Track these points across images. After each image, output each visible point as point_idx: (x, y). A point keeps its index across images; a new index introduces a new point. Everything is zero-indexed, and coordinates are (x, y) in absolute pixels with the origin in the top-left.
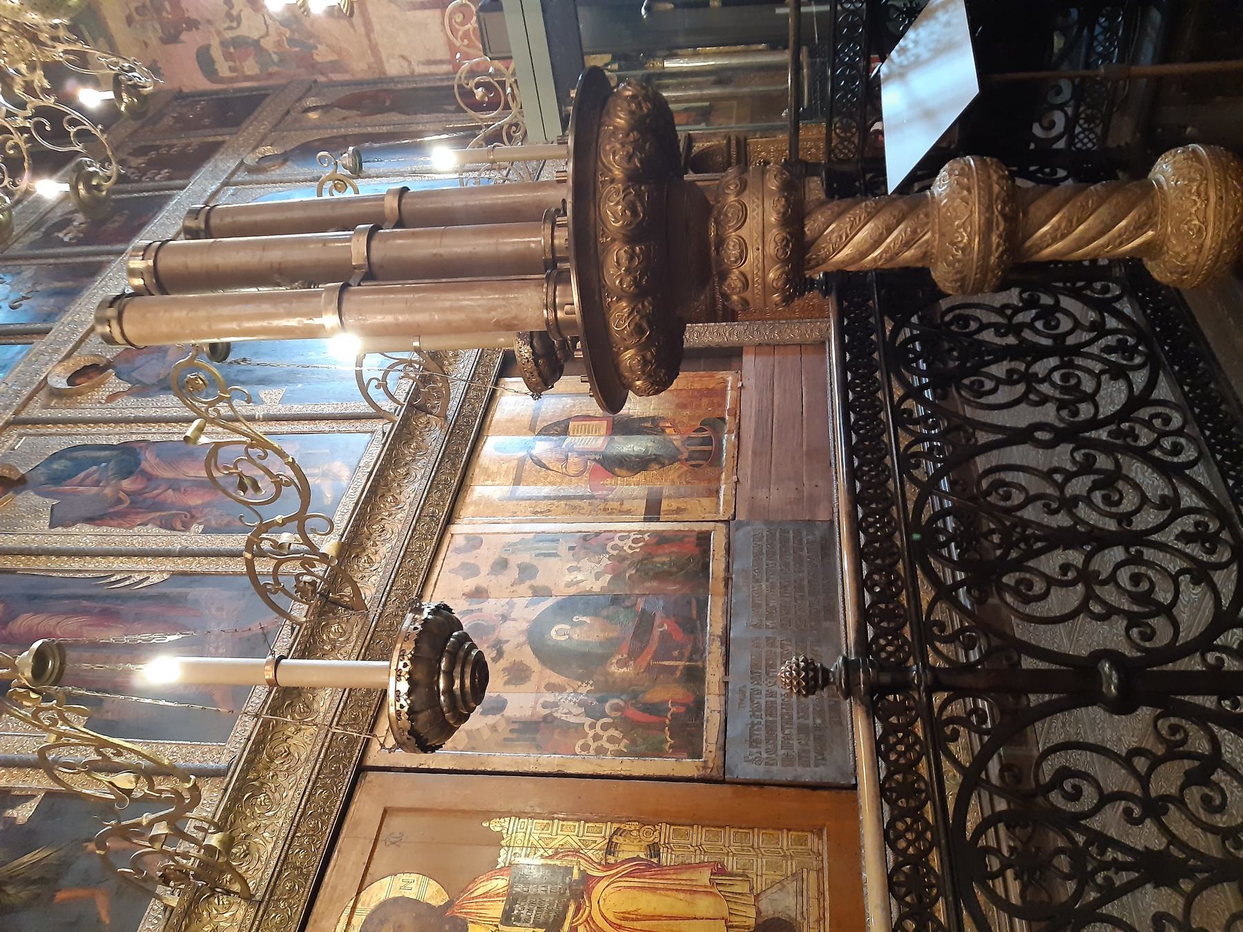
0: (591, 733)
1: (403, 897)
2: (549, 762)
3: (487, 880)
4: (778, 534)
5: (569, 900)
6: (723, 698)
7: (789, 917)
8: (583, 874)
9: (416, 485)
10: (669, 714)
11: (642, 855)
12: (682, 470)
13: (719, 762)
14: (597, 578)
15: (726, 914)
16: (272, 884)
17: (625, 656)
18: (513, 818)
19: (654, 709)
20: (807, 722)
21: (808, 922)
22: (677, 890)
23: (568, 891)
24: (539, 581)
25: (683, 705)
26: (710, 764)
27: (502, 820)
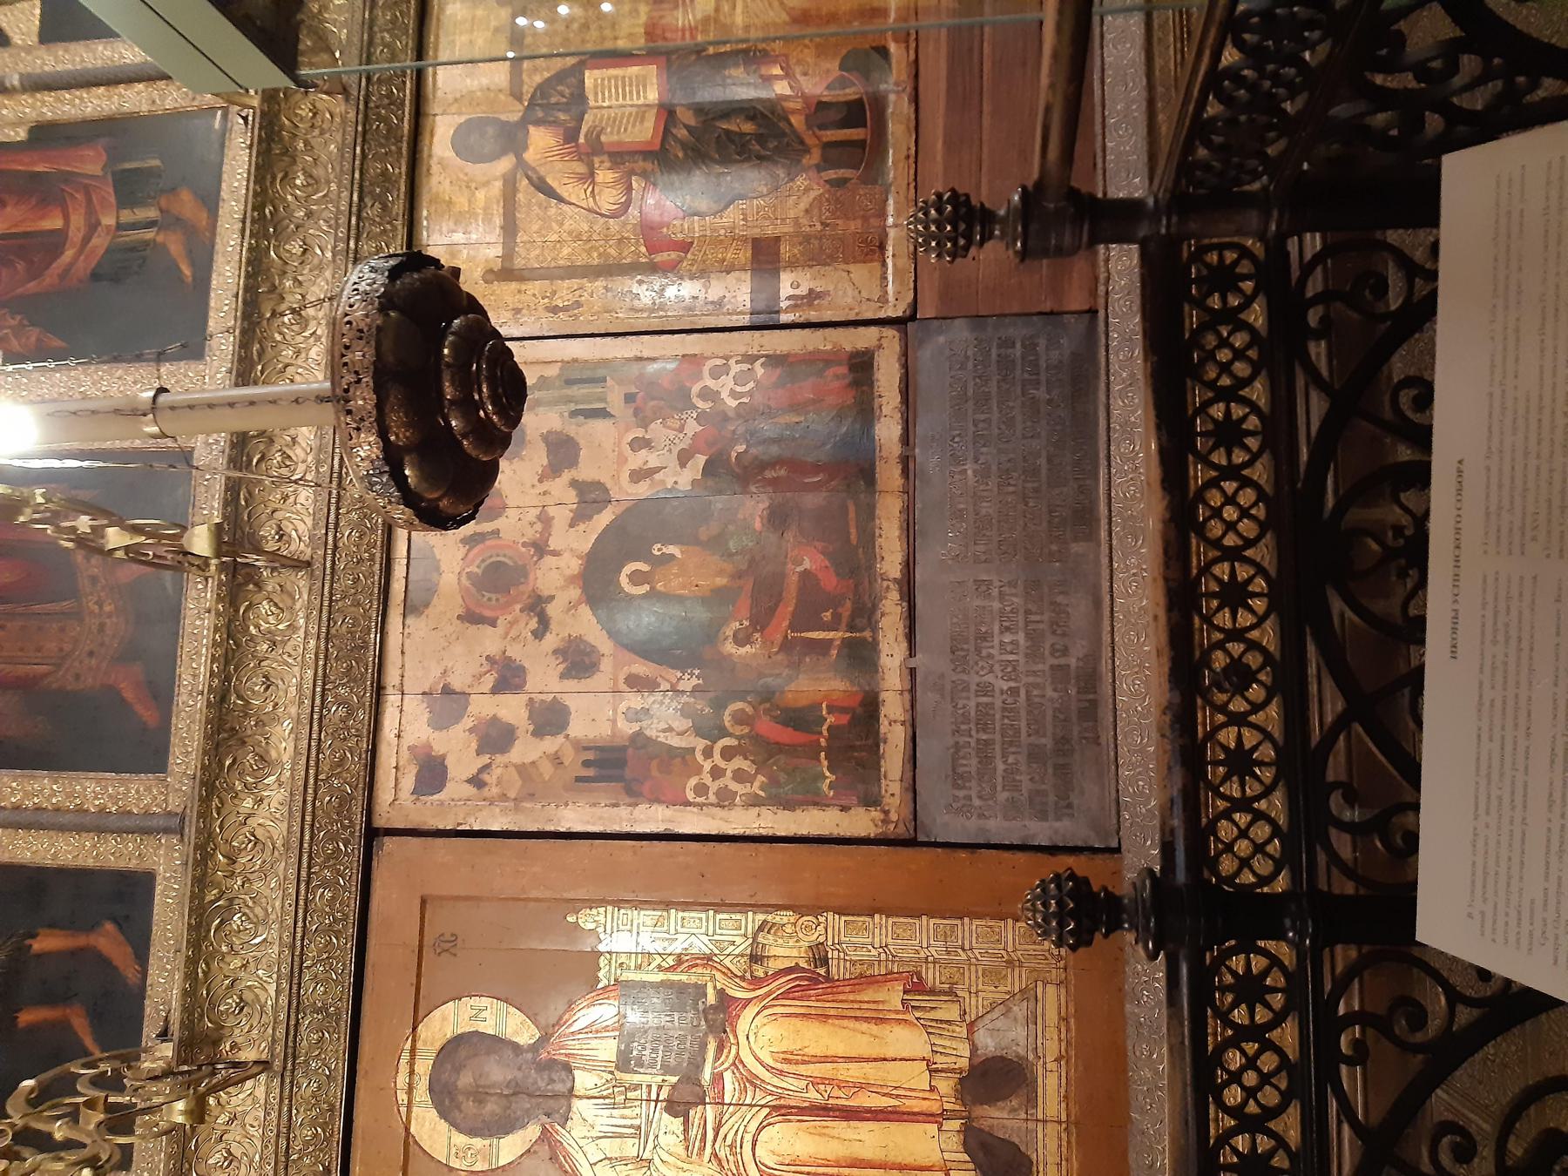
0: (707, 766)
1: (477, 1033)
2: (652, 818)
3: (588, 1006)
4: (994, 352)
5: (706, 1035)
6: (907, 696)
7: (1018, 1056)
8: (721, 993)
9: (328, 274)
10: (825, 727)
11: (803, 965)
12: (813, 194)
13: (907, 812)
14: (683, 465)
15: (927, 1052)
16: (290, 1044)
17: (746, 623)
18: (610, 908)
19: (800, 719)
20: (1043, 741)
21: (1045, 1063)
22: (856, 1018)
23: (703, 1023)
24: (586, 471)
25: (843, 710)
26: (894, 817)
27: (594, 911)
